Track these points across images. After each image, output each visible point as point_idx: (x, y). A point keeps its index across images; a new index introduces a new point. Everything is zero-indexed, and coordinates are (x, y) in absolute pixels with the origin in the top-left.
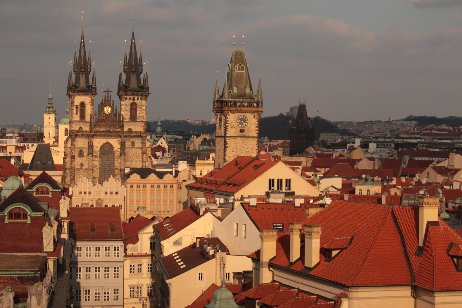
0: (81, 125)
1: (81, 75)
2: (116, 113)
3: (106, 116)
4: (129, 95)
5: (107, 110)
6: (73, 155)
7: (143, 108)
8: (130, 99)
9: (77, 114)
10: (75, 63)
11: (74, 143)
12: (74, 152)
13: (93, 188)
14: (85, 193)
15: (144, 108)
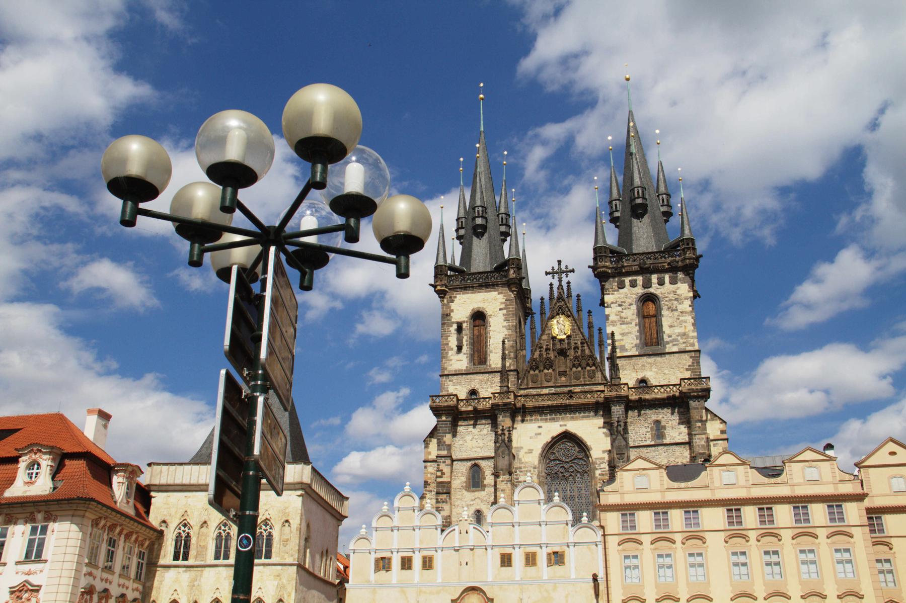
0: (476, 382)
1: (475, 239)
2: (591, 336)
3: (558, 346)
4: (628, 274)
5: (561, 327)
6: (445, 479)
7: (680, 307)
8: (633, 284)
9: (460, 348)
10: (462, 214)
11: (448, 438)
12: (447, 470)
13: (439, 539)
14: (406, 563)
15: (686, 306)
